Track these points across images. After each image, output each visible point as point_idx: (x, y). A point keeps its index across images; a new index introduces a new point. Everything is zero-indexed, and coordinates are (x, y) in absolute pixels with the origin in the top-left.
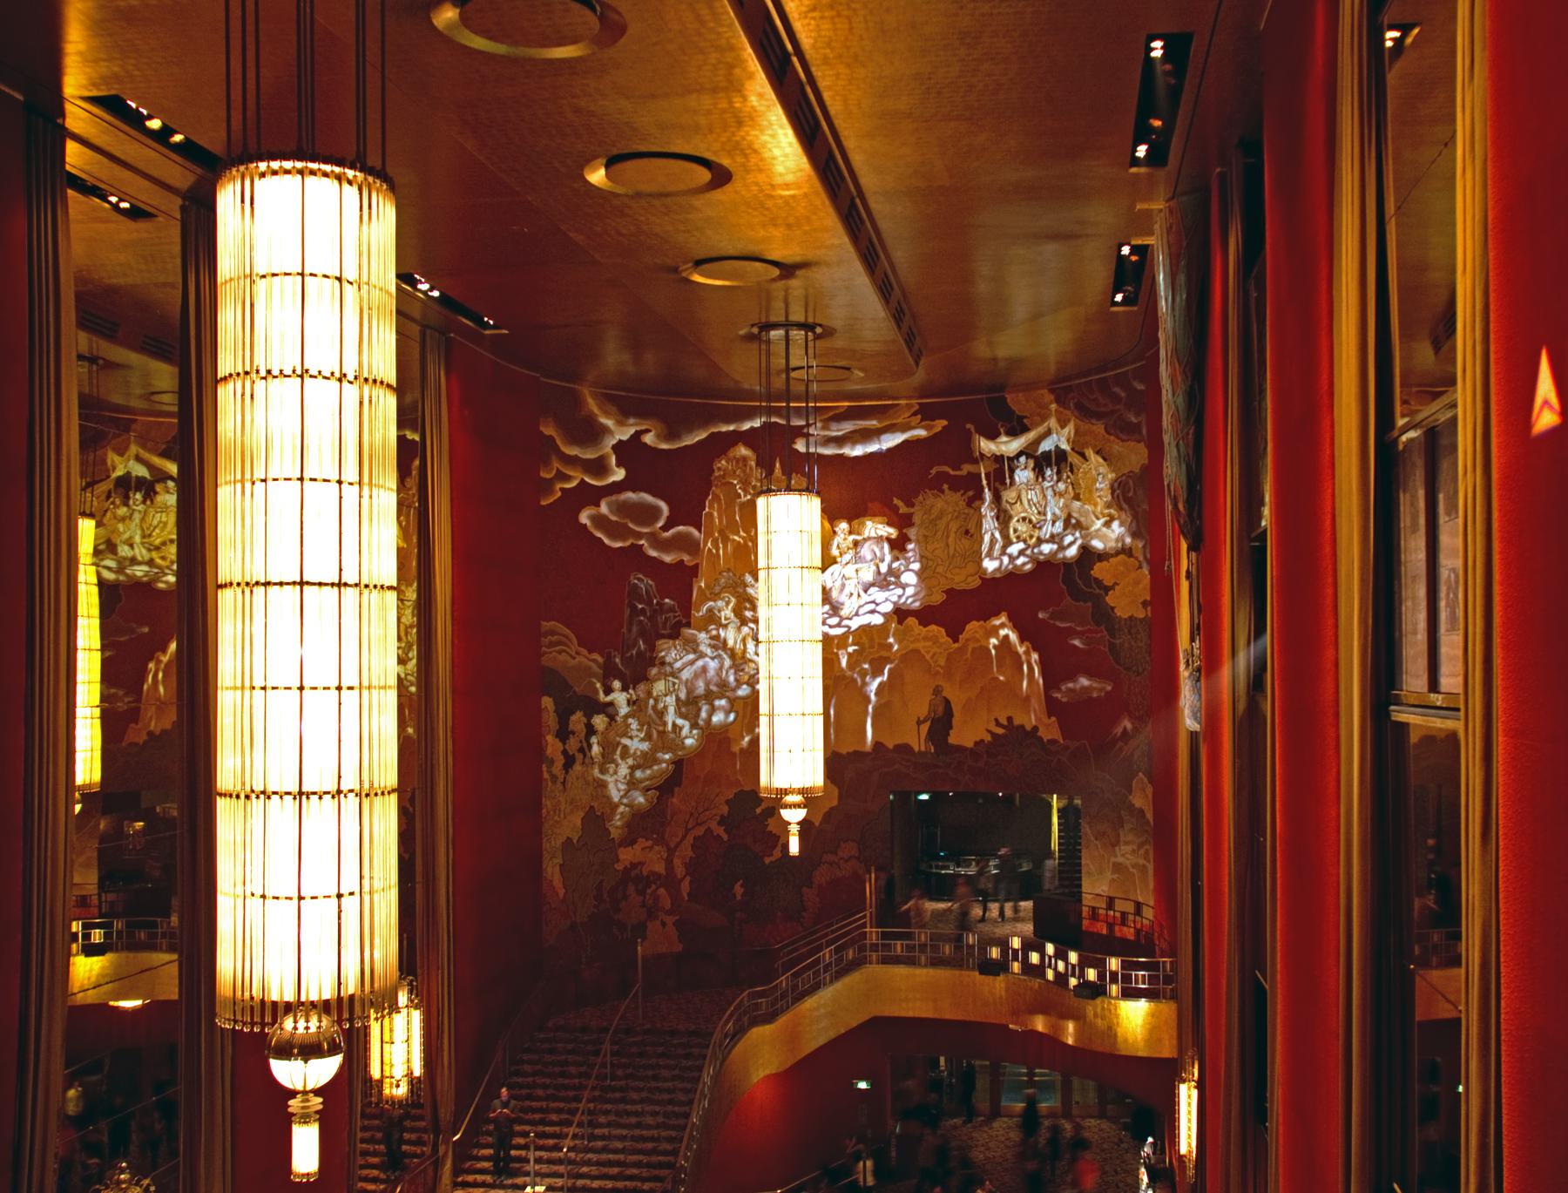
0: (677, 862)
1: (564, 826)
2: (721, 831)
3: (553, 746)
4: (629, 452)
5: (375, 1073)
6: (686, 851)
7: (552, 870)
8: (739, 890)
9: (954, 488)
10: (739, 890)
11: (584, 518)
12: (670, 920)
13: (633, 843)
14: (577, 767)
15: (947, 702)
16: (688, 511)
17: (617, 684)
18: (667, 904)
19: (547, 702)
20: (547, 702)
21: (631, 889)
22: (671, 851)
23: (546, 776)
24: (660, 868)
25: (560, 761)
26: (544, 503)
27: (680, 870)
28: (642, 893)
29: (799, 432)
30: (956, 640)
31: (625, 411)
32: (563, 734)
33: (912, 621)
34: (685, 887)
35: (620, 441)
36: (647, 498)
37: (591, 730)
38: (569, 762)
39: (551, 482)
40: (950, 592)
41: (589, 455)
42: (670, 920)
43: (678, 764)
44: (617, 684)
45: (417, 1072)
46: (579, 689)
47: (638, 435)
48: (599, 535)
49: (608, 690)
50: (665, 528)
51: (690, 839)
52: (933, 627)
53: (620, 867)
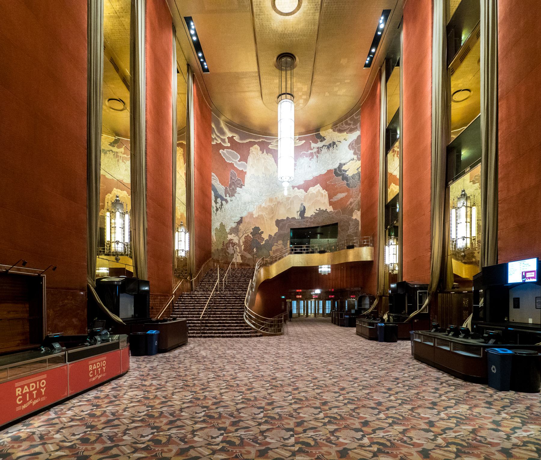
0: (241, 241)
1: (215, 225)
2: (251, 235)
3: (213, 204)
4: (231, 139)
6: (243, 239)
7: (213, 233)
8: (255, 250)
9: (307, 157)
10: (255, 250)
12: (239, 255)
13: (231, 234)
14: (219, 212)
15: (304, 207)
16: (244, 159)
17: (228, 195)
18: (238, 250)
21: (231, 245)
22: (240, 238)
25: (215, 208)
27: (242, 244)
28: (233, 247)
29: (269, 143)
30: (306, 192)
31: (231, 130)
32: (216, 202)
33: (296, 188)
34: (243, 248)
37: (222, 205)
38: (217, 210)
40: (305, 181)
41: (222, 137)
42: (239, 255)
43: (242, 218)
44: (228, 195)
46: (220, 193)
47: (233, 137)
49: (226, 196)
50: (239, 161)
52: (301, 190)
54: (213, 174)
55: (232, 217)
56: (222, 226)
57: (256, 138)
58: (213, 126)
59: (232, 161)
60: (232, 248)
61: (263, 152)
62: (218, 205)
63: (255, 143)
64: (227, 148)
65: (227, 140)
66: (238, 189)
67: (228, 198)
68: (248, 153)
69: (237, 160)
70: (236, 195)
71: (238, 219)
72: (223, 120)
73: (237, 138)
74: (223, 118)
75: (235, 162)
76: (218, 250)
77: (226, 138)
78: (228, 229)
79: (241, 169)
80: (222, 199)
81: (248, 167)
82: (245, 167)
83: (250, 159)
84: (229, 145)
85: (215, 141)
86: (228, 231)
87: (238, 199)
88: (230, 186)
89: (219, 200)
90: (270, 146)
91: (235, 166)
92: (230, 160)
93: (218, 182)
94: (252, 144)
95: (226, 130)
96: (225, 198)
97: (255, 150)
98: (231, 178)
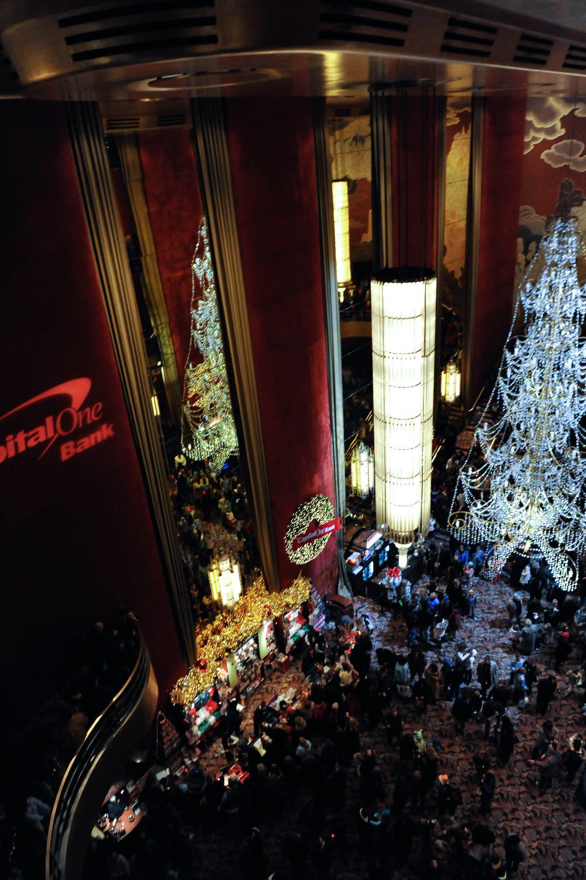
3: (521, 258)
4: (566, 121)
5: (443, 394)
11: (543, 156)
19: (520, 240)
20: (520, 240)
23: (517, 270)
25: (524, 263)
26: (525, 153)
35: (564, 117)
36: (575, 141)
38: (528, 263)
39: (529, 142)
45: (458, 394)
46: (535, 232)
47: (574, 110)
48: (549, 163)
59: (570, 160)
69: (577, 156)
77: (557, 123)
91: (572, 168)
92: (561, 159)
93: (534, 215)
98: (561, 193)
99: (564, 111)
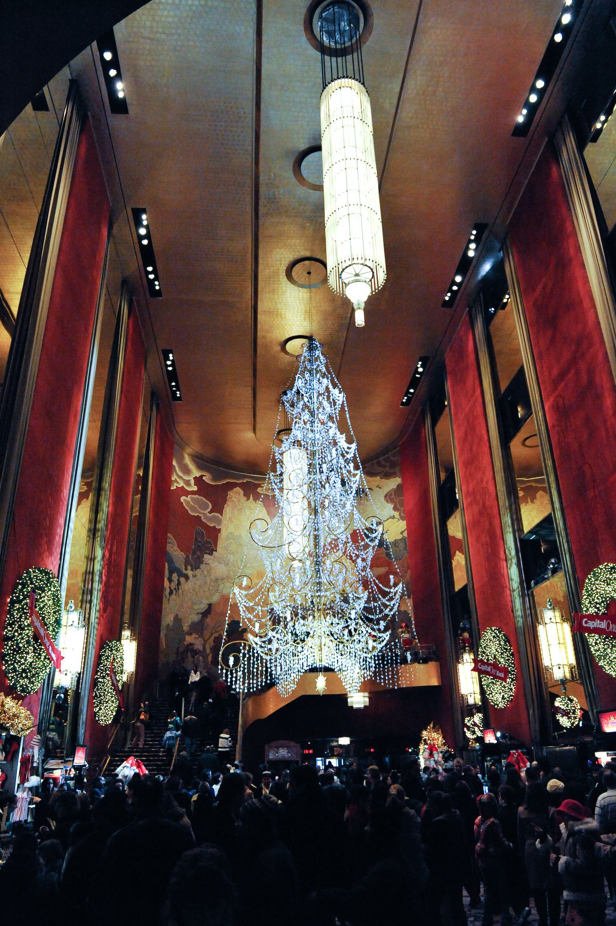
0: (208, 647)
1: (168, 619)
4: (199, 481)
7: (162, 635)
13: (191, 634)
14: (173, 596)
16: (218, 508)
17: (189, 567)
22: (205, 641)
24: (200, 648)
25: (167, 592)
27: (208, 651)
29: (259, 486)
31: (200, 467)
32: (170, 580)
37: (179, 584)
38: (171, 593)
41: (186, 478)
43: (210, 605)
44: (189, 567)
46: (177, 565)
47: (202, 476)
49: (186, 569)
50: (210, 512)
51: (213, 638)
53: (186, 643)
54: (169, 535)
55: (194, 603)
56: (177, 619)
57: (238, 479)
58: (174, 463)
60: (190, 659)
61: (248, 499)
62: (173, 586)
63: (235, 485)
64: (193, 493)
65: (192, 482)
66: (206, 556)
67: (190, 573)
68: (224, 501)
70: (202, 566)
71: (203, 607)
72: (189, 455)
73: (207, 478)
74: (189, 450)
75: (204, 515)
76: (167, 663)
78: (187, 625)
79: (212, 525)
80: (181, 574)
81: (224, 522)
82: (219, 522)
83: (227, 509)
84: (195, 488)
85: (175, 484)
86: (185, 628)
87: (205, 573)
88: (194, 553)
89: (175, 576)
90: (259, 490)
93: (176, 547)
94: (231, 486)
95: (192, 466)
96: (184, 572)
97: (236, 495)
98: (196, 539)
99: (197, 473)
